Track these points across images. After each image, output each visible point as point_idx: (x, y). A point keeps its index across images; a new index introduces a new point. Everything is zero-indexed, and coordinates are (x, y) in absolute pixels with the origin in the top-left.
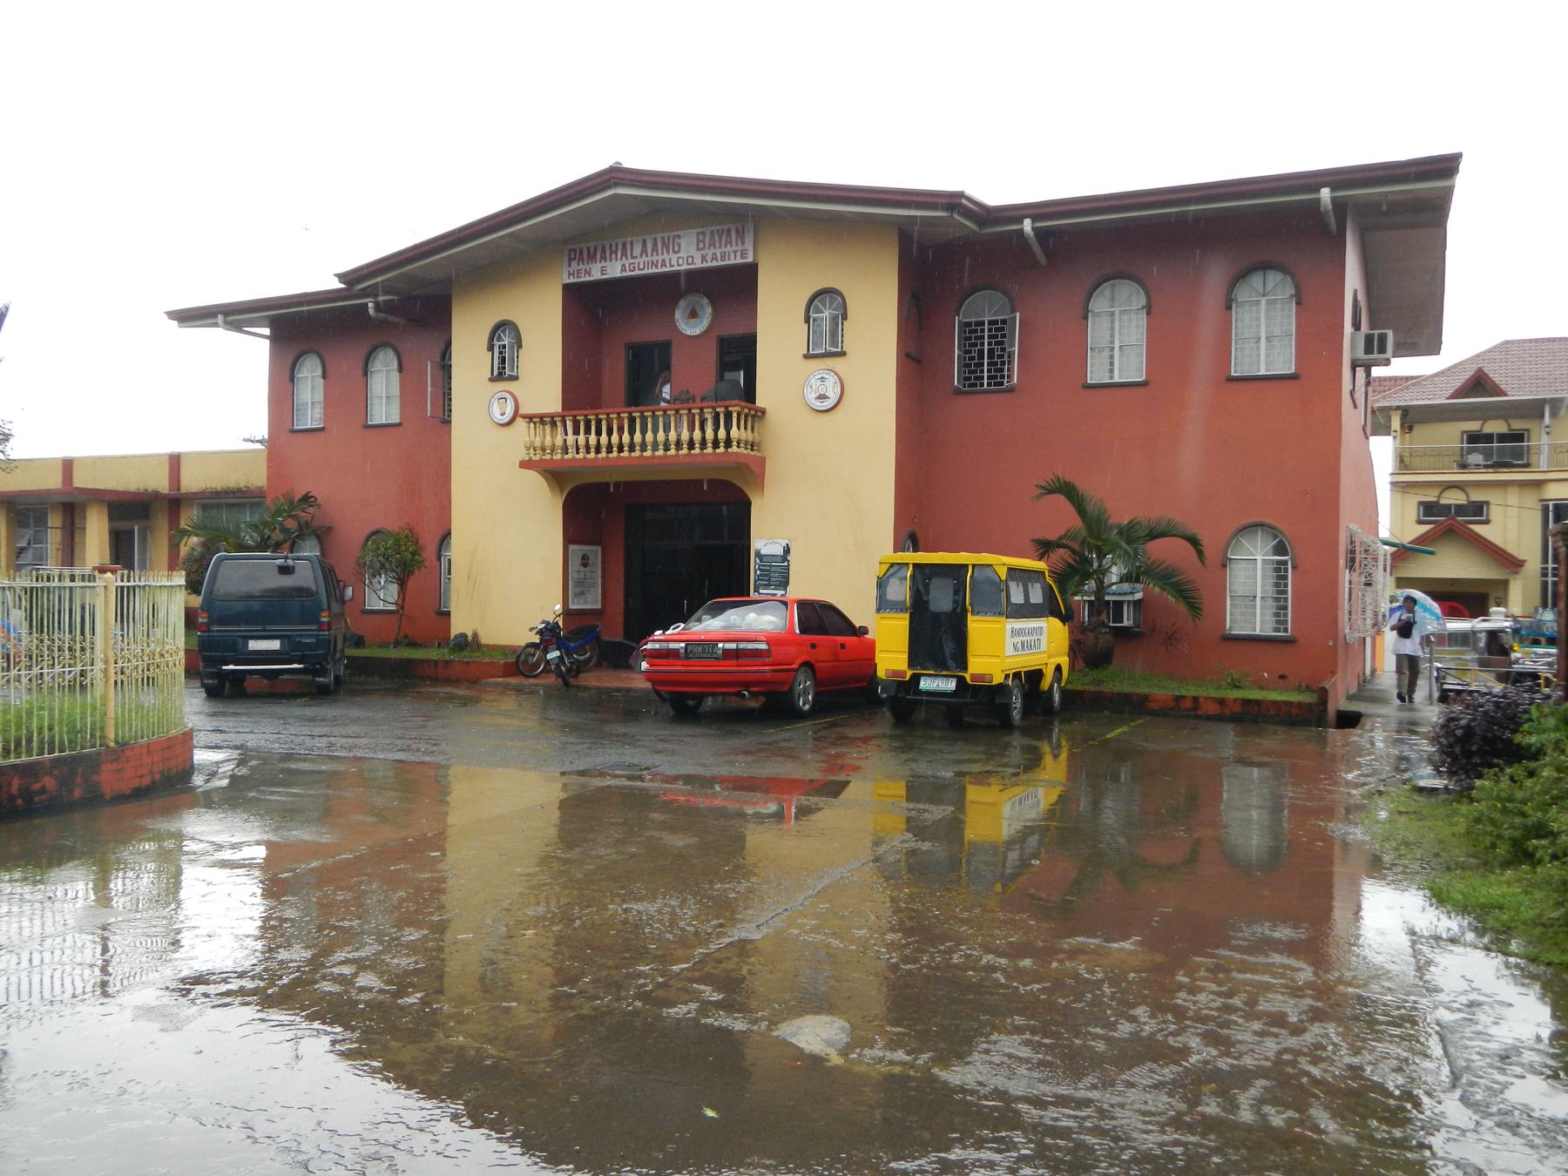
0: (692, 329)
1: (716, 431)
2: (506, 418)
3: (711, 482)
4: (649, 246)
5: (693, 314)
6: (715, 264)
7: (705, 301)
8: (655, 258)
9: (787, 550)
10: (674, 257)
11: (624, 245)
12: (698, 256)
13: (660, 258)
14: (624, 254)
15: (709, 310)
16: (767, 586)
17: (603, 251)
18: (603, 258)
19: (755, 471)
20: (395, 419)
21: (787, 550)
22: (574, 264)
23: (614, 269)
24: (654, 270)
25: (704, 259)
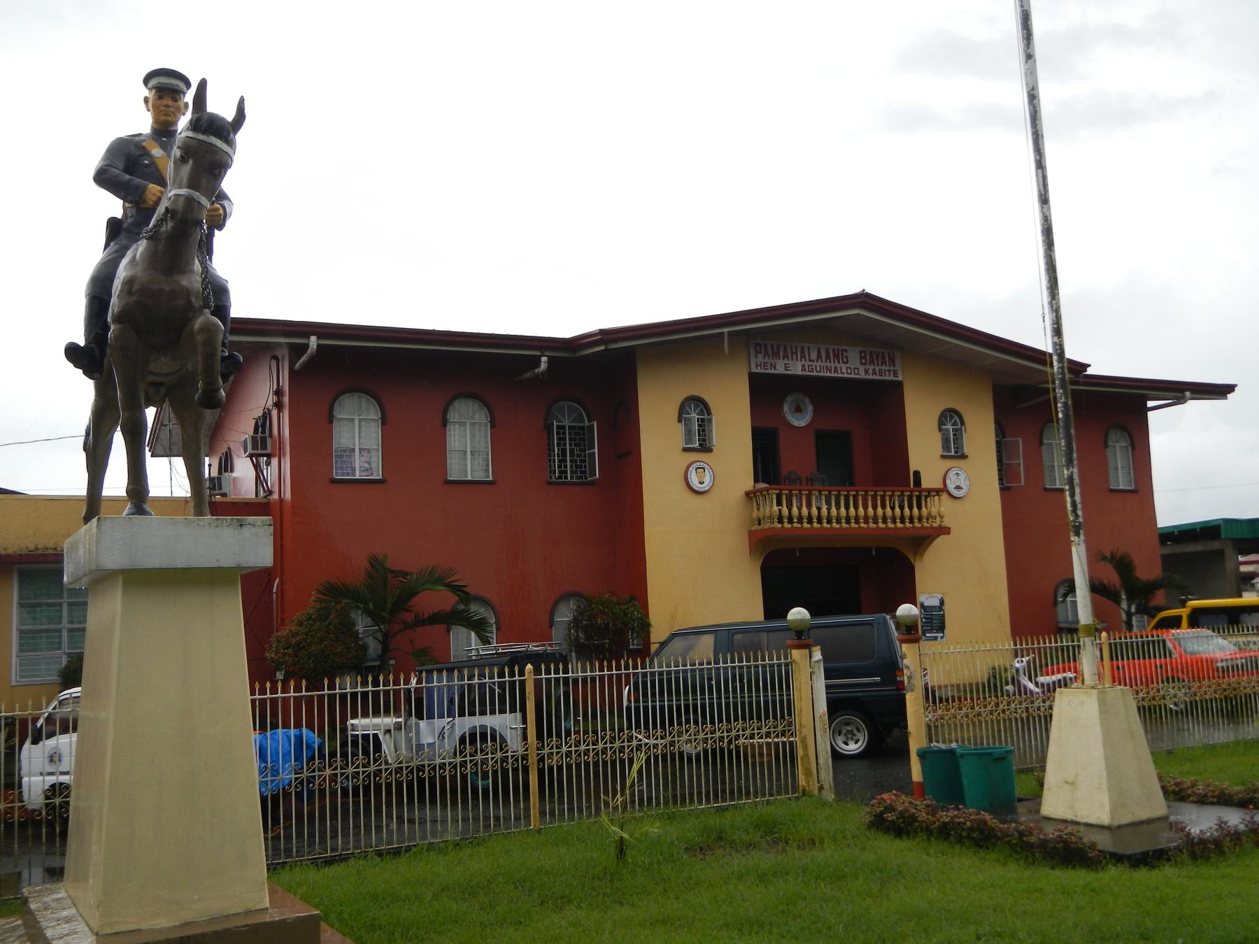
0: (800, 421)
1: (800, 509)
2: (705, 487)
3: (877, 549)
4: (823, 353)
5: (798, 410)
6: (875, 377)
7: (807, 400)
8: (828, 364)
9: (942, 602)
10: (844, 367)
11: (803, 349)
12: (862, 369)
13: (833, 365)
14: (803, 356)
15: (810, 408)
16: (930, 631)
17: (785, 351)
18: (786, 356)
19: (923, 540)
20: (480, 476)
21: (942, 602)
22: (760, 356)
23: (796, 368)
24: (828, 374)
25: (866, 371)
